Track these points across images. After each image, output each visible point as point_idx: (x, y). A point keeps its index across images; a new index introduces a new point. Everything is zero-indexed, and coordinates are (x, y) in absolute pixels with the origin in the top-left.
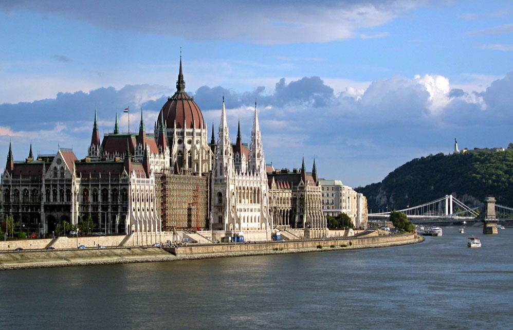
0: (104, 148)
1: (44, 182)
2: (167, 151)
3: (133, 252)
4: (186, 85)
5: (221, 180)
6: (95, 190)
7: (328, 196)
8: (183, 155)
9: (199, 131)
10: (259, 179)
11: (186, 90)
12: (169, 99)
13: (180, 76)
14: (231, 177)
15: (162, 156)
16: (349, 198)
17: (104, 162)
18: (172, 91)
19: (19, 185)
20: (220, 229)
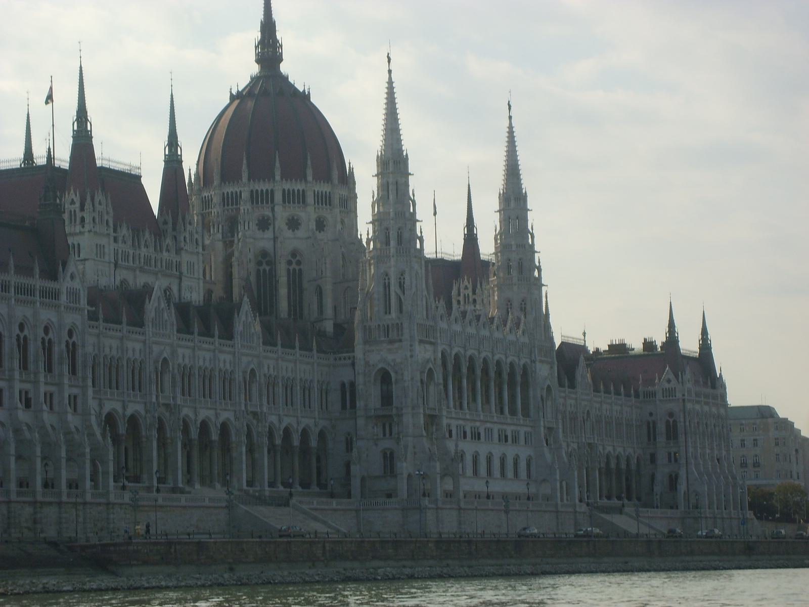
5: (387, 330)
7: (743, 445)
8: (272, 263)
9: (325, 188)
11: (284, 68)
12: (232, 96)
15: (169, 241)
16: (797, 451)
18: (243, 69)
20: (389, 496)
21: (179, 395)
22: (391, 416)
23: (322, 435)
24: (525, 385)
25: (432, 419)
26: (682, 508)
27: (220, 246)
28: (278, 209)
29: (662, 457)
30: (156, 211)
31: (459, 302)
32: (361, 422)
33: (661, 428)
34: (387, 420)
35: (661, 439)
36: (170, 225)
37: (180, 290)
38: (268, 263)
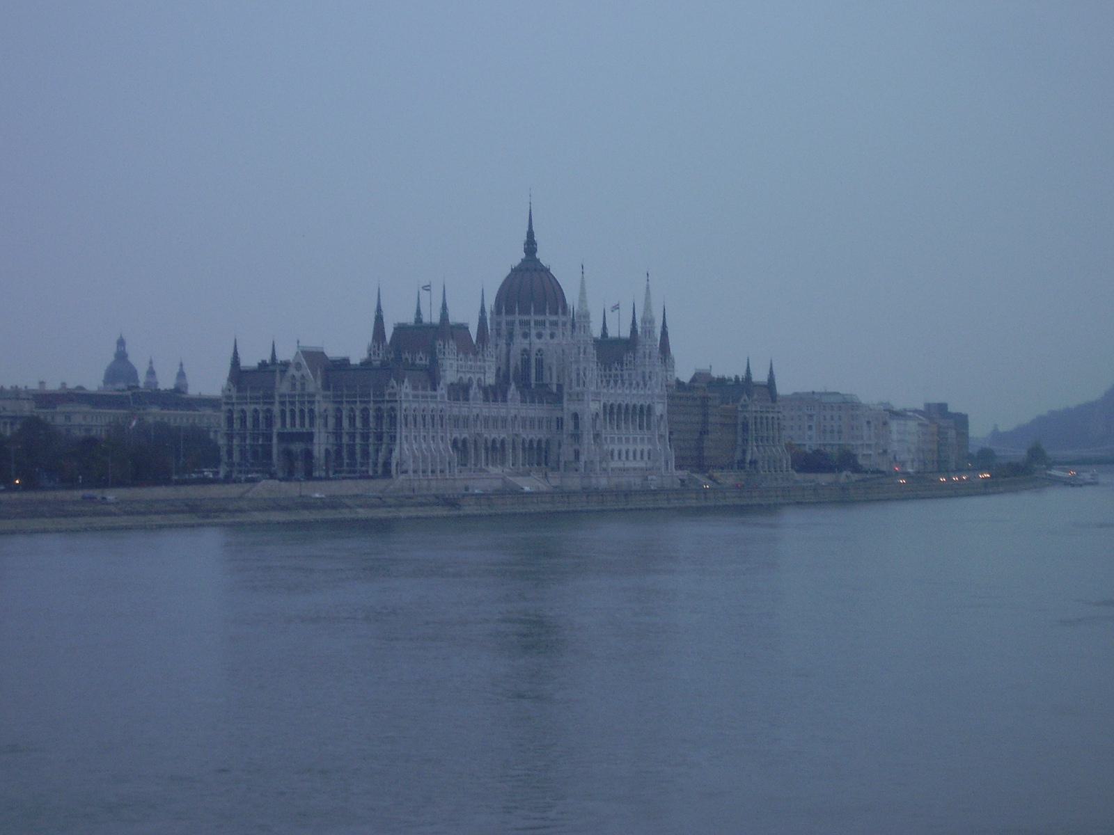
1: (277, 398)
3: (385, 502)
6: (352, 410)
7: (832, 419)
8: (528, 355)
9: (554, 318)
11: (537, 256)
13: (530, 234)
15: (480, 357)
16: (868, 423)
18: (518, 256)
19: (246, 403)
21: (483, 429)
23: (548, 442)
27: (504, 346)
30: (474, 341)
31: (627, 364)
32: (565, 436)
34: (576, 437)
36: (481, 349)
37: (485, 379)
38: (527, 355)
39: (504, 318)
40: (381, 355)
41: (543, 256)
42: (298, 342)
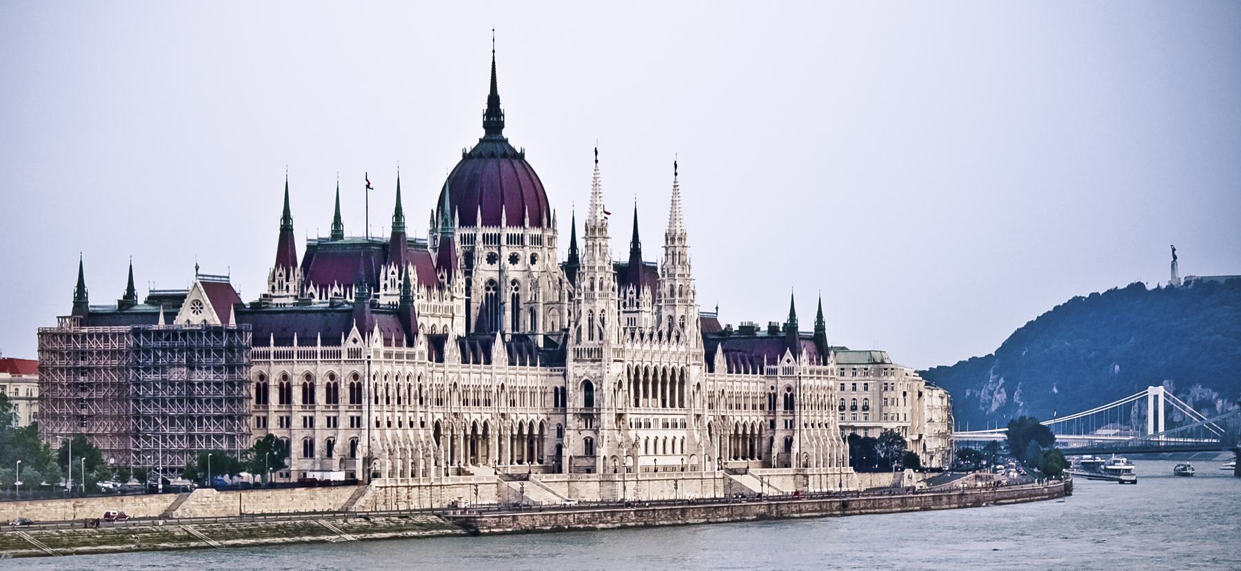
0: (305, 274)
2: (460, 281)
3: (375, 524)
4: (508, 120)
5: (590, 352)
7: (854, 389)
9: (537, 232)
10: (682, 348)
11: (505, 133)
12: (464, 155)
13: (494, 100)
14: (614, 341)
15: (447, 292)
16: (905, 394)
17: (307, 308)
20: (589, 471)
22: (592, 415)
24: (682, 383)
25: (620, 417)
26: (794, 467)
28: (504, 249)
29: (780, 424)
32: (569, 417)
33: (781, 400)
34: (589, 416)
35: (780, 409)
39: (458, 232)
40: (291, 288)
41: (513, 134)
42: (197, 268)
